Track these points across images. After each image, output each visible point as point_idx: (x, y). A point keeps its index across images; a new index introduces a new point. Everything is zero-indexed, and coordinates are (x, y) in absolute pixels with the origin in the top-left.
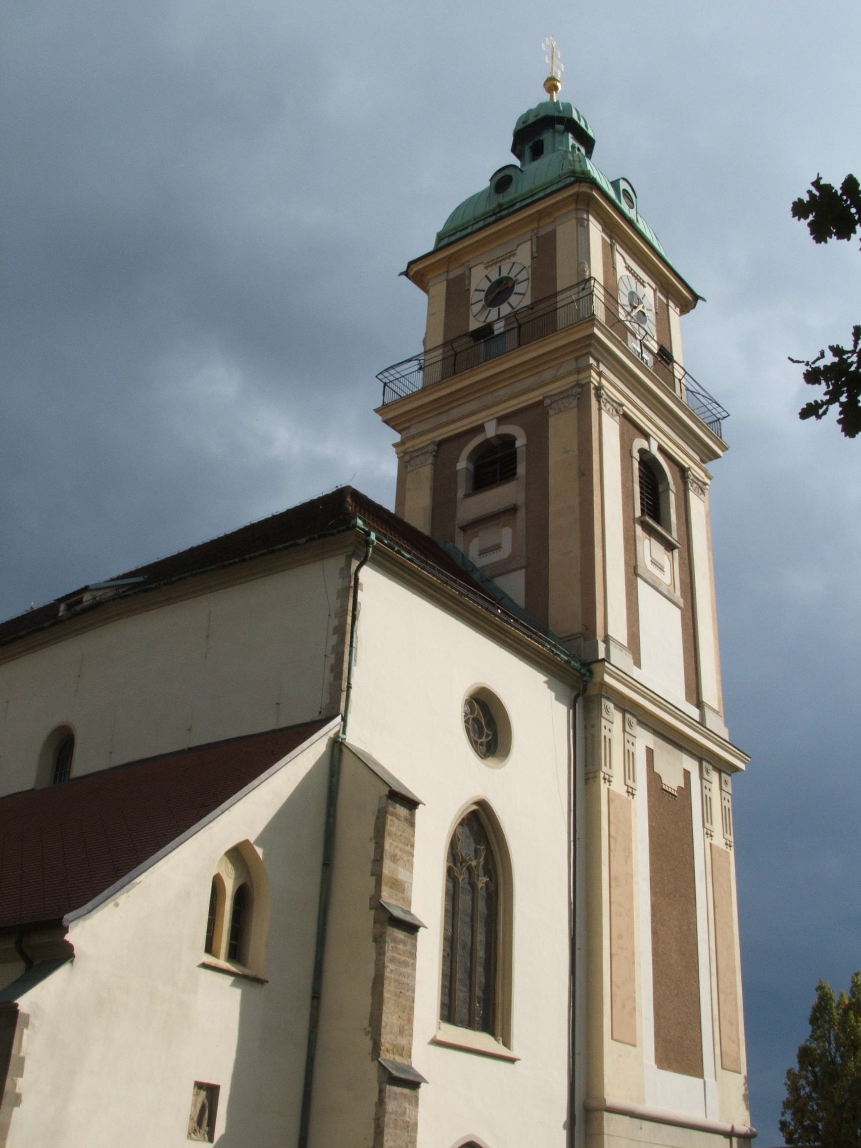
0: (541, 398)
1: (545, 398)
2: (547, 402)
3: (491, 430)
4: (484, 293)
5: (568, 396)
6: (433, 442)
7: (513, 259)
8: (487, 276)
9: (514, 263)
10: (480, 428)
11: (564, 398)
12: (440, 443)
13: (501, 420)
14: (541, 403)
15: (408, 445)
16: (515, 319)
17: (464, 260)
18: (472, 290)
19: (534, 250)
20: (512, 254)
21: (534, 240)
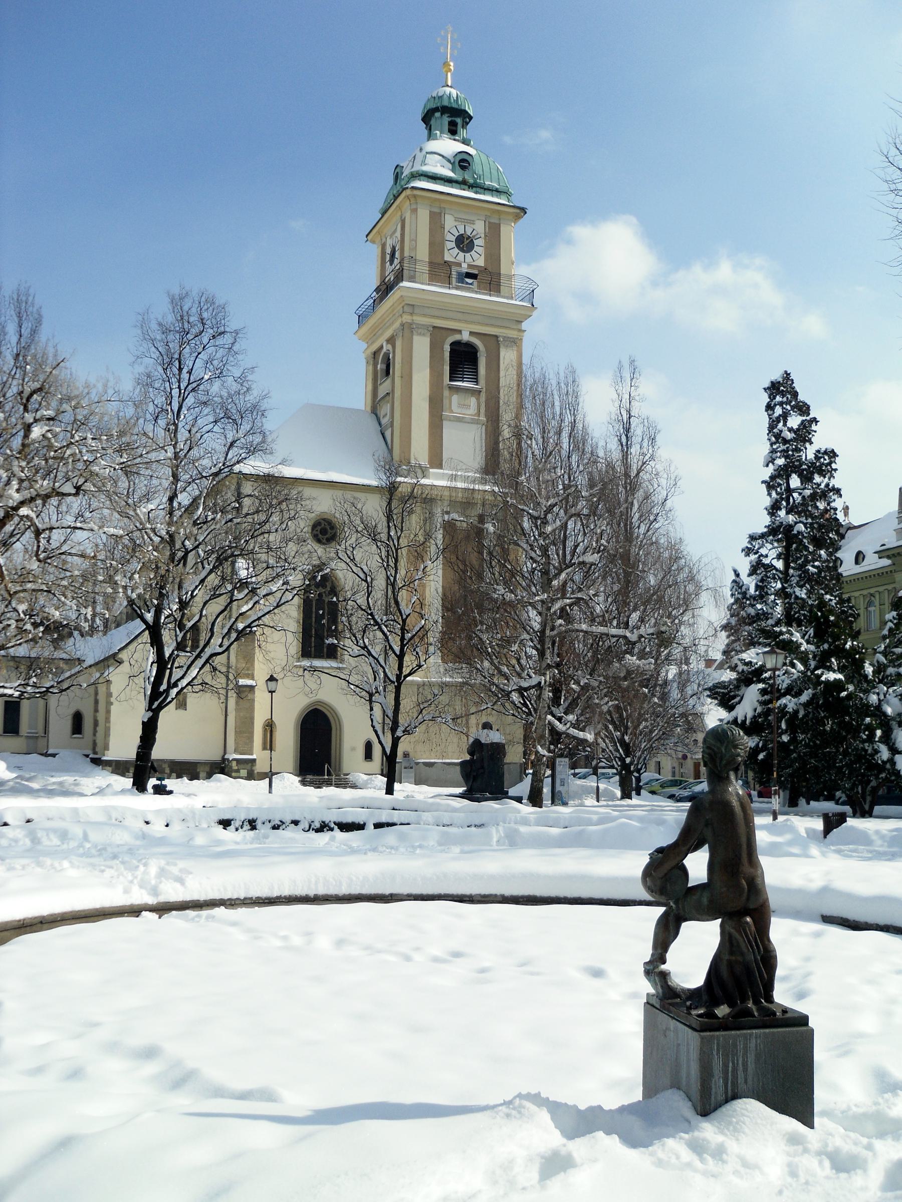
3: (465, 337)
7: (472, 225)
10: (460, 332)
12: (434, 327)
13: (471, 333)
14: (497, 337)
15: (415, 318)
18: (446, 231)
20: (472, 222)
21: (487, 223)
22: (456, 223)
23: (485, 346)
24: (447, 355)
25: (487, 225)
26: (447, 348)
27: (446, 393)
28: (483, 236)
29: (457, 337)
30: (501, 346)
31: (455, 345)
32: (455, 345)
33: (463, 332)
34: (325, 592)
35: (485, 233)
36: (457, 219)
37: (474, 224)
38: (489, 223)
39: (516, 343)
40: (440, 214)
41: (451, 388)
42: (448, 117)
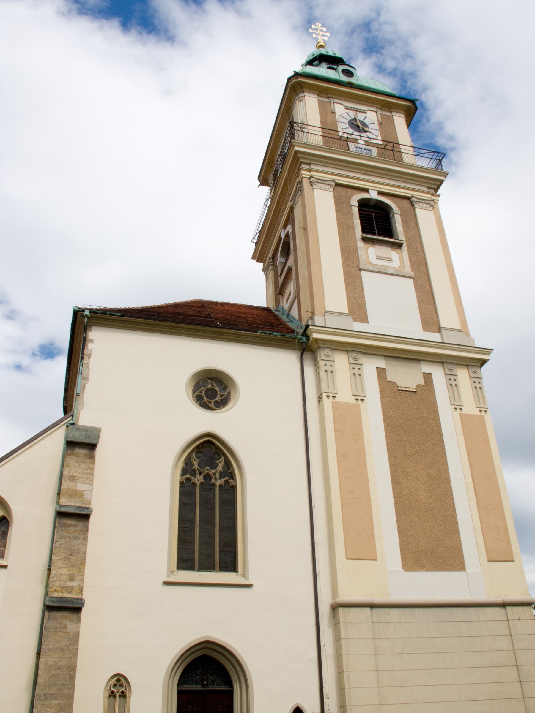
0: (410, 196)
1: (413, 196)
2: (413, 199)
3: (373, 195)
4: (348, 121)
5: (427, 204)
6: (334, 181)
7: (363, 114)
8: (347, 113)
9: (366, 117)
10: (366, 191)
11: (425, 203)
12: (337, 185)
13: (380, 193)
14: (408, 198)
16: (394, 148)
17: (329, 95)
18: (337, 115)
19: (380, 118)
22: (348, 111)
23: (399, 207)
24: (355, 211)
25: (379, 115)
26: (354, 202)
27: (361, 244)
28: (377, 122)
29: (365, 195)
30: (416, 206)
31: (364, 204)
32: (364, 204)
33: (370, 191)
34: (215, 474)
35: (378, 121)
36: (347, 108)
37: (366, 113)
38: (380, 114)
39: (432, 205)
40: (330, 102)
41: (364, 239)
42: (326, 64)
